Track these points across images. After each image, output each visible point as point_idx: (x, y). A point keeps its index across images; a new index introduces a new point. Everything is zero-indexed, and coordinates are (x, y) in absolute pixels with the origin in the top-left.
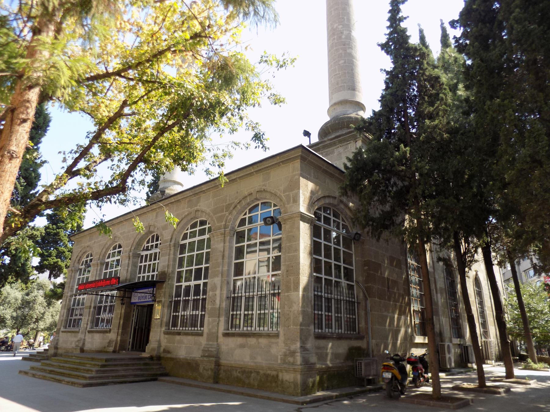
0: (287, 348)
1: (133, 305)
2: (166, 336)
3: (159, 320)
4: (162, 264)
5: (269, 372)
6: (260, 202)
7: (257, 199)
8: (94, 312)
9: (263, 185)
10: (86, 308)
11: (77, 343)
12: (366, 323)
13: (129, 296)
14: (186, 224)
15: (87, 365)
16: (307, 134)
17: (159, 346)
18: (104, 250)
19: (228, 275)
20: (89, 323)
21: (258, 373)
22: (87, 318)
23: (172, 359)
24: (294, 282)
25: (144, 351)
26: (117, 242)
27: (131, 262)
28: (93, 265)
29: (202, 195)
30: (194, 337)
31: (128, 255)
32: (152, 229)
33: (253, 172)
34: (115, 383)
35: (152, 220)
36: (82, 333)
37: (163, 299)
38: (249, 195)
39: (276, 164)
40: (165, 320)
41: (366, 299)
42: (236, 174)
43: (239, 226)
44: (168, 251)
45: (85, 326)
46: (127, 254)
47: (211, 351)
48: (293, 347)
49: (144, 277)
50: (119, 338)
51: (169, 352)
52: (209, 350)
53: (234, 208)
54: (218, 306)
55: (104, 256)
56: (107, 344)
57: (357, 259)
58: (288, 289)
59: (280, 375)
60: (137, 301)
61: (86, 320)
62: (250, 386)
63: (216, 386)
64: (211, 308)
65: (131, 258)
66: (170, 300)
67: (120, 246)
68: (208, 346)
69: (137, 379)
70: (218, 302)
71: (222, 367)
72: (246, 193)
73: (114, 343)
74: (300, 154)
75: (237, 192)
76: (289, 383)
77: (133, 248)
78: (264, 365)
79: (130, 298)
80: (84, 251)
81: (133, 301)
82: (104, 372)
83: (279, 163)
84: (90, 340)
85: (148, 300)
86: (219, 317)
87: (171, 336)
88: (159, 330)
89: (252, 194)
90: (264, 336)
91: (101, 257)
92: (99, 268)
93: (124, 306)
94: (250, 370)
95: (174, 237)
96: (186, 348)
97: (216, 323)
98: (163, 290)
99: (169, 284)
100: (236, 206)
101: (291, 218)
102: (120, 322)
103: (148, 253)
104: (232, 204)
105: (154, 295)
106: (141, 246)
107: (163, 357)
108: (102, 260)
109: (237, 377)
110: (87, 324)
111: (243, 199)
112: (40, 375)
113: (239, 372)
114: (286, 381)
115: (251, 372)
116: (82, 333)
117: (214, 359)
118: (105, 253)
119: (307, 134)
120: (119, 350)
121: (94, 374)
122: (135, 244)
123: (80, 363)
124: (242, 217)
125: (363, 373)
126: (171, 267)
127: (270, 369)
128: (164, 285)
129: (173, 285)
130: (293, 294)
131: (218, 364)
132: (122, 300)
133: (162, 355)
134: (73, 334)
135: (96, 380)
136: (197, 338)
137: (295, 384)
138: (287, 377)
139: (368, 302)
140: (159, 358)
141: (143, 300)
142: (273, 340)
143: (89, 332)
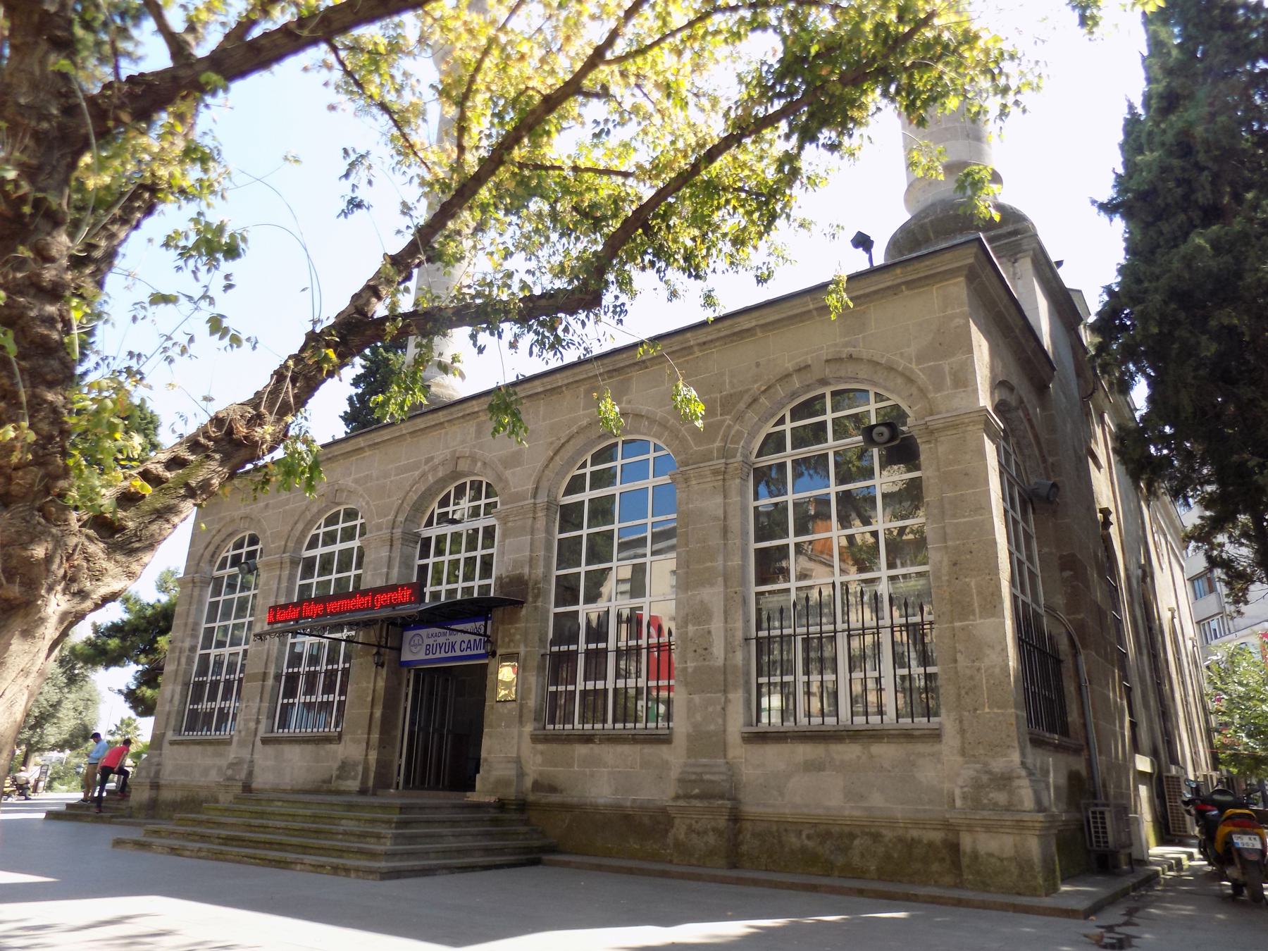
0: (978, 766)
1: (406, 670)
2: (540, 747)
3: (514, 705)
4: (508, 556)
5: (915, 833)
6: (827, 391)
7: (824, 382)
8: (275, 690)
9: (846, 345)
10: (252, 678)
11: (230, 772)
12: (1083, 714)
13: (395, 644)
14: (580, 452)
15: (343, 822)
16: (863, 242)
17: (521, 774)
18: (300, 526)
19: (744, 582)
20: (263, 719)
21: (876, 837)
22: (255, 705)
23: (566, 807)
24: (980, 593)
25: (472, 787)
26: (339, 504)
27: (397, 554)
28: (268, 565)
29: (635, 374)
30: (638, 747)
31: (388, 536)
32: (463, 466)
33: (810, 311)
34: (452, 870)
35: (463, 442)
36: (242, 744)
37: (522, 650)
38: (799, 370)
39: (888, 288)
40: (532, 703)
41: (1075, 655)
42: (755, 314)
43: (759, 455)
44: (530, 521)
45: (252, 725)
46: (385, 533)
47: (712, 782)
48: (998, 765)
49: (451, 593)
50: (373, 756)
51: (553, 789)
52: (702, 781)
53: (749, 405)
54: (720, 662)
55: (299, 542)
56: (335, 773)
57: (1046, 550)
58: (961, 608)
59: (966, 841)
60: (421, 656)
61: (255, 711)
62: (860, 874)
63: (734, 873)
64: (696, 669)
65: (397, 544)
66: (542, 651)
67: (351, 514)
68: (699, 770)
69: (498, 859)
70: (718, 650)
71: (748, 825)
72: (790, 366)
73: (360, 769)
74: (971, 260)
75: (758, 365)
76: (1001, 860)
77: (401, 518)
78: (899, 816)
79: (399, 649)
80: (230, 530)
81: (407, 656)
82: (412, 839)
83: (899, 285)
84: (270, 763)
85: (458, 653)
86: (725, 691)
87: (556, 747)
88: (515, 731)
89: (808, 367)
90: (888, 736)
91: (291, 544)
92: (286, 573)
93: (384, 672)
94: (847, 829)
95: (545, 484)
96: (605, 776)
97: (719, 708)
98: (521, 625)
99: (536, 608)
100: (755, 400)
101: (955, 426)
102: (372, 714)
103: (448, 530)
104: (742, 394)
105: (489, 640)
106: (424, 513)
107: (536, 805)
108: (294, 551)
109: (803, 850)
110: (258, 722)
111: (780, 380)
112: (200, 850)
113: (809, 837)
114: (990, 855)
115: (852, 836)
116: (242, 744)
117: (728, 804)
118: (303, 534)
119: (863, 242)
120: (376, 786)
121: (388, 846)
122: (407, 507)
123: (314, 816)
124: (769, 428)
125: (1110, 839)
126: (541, 563)
127: (917, 824)
128: (524, 612)
129: (548, 611)
130: (981, 625)
131: (736, 817)
132: (378, 653)
133: (531, 798)
134: (210, 749)
135: (401, 860)
136: (648, 750)
137: (1024, 864)
138: (992, 845)
139: (1082, 659)
140: (523, 806)
141: (443, 655)
142: (921, 748)
143: (265, 741)
